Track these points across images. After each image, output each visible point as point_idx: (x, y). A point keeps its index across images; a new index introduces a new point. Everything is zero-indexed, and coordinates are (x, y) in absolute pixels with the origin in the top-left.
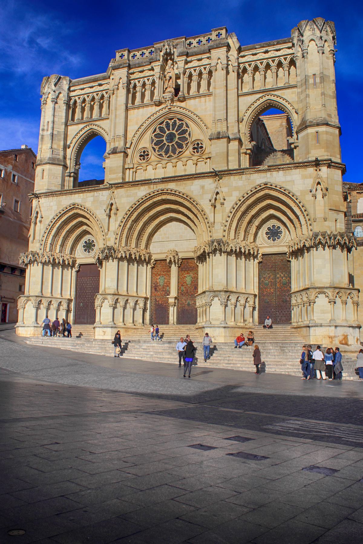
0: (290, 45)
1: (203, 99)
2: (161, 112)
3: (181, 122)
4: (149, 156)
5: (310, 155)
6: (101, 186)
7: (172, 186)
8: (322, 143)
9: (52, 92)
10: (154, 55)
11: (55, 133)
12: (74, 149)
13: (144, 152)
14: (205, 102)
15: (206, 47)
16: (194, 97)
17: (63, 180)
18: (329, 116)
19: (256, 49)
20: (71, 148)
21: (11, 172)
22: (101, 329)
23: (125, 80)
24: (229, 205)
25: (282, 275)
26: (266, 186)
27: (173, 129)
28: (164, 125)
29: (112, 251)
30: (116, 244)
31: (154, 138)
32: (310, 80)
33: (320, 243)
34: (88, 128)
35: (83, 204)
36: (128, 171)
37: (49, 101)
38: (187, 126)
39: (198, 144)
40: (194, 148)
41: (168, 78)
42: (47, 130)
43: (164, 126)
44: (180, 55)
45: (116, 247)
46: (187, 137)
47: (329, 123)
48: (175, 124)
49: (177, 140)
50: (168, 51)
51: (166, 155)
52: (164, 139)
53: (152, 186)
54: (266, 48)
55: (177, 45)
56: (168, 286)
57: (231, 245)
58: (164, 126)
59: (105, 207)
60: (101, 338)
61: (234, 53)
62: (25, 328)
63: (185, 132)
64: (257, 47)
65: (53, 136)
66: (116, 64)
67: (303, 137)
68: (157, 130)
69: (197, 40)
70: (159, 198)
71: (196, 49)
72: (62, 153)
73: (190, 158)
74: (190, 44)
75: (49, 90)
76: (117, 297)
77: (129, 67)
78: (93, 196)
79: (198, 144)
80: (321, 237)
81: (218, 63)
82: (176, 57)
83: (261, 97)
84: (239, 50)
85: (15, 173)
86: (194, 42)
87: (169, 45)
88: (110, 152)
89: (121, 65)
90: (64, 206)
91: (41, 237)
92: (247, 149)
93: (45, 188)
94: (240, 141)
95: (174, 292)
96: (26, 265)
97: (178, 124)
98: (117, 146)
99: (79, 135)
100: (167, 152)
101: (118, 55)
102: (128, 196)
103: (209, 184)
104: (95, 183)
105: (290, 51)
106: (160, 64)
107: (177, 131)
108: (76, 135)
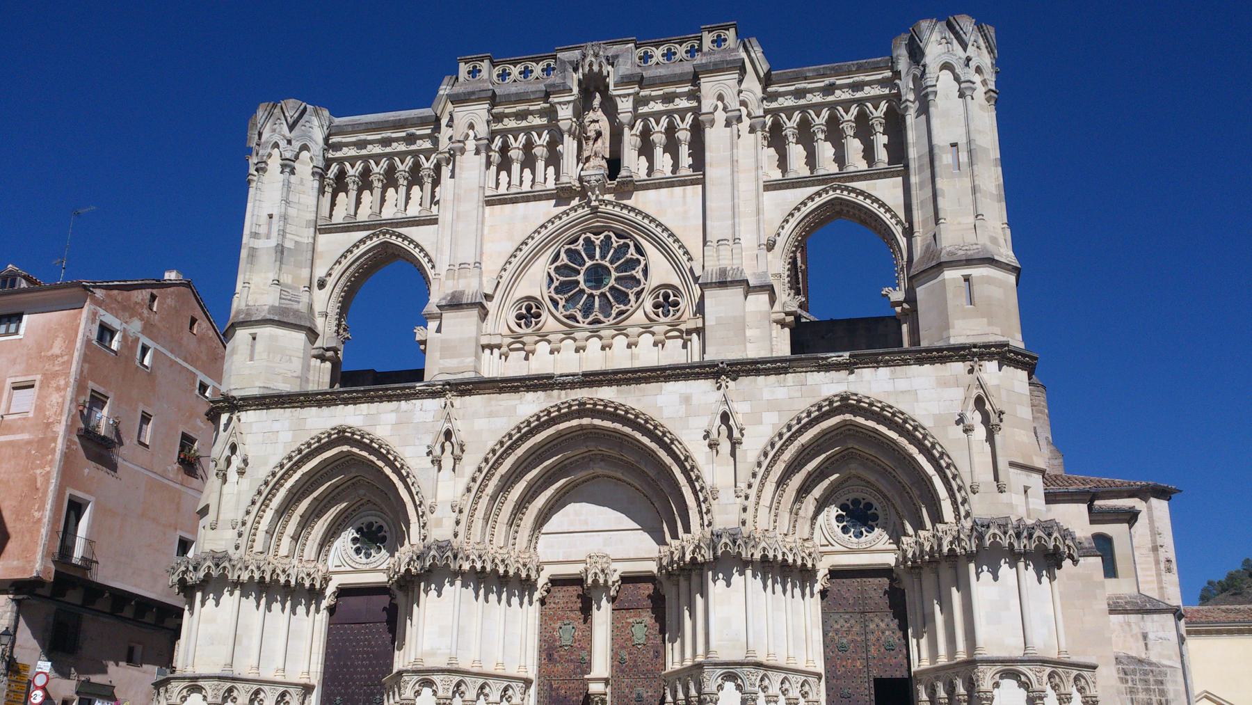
0: (888, 74)
2: (572, 214)
3: (622, 241)
4: (543, 318)
5: (952, 332)
6: (419, 386)
7: (607, 393)
8: (982, 305)
9: (283, 144)
10: (555, 78)
11: (288, 244)
12: (337, 290)
13: (529, 309)
14: (684, 197)
15: (688, 67)
17: (306, 368)
18: (994, 240)
20: (329, 287)
21: (137, 339)
23: (482, 130)
24: (754, 444)
25: (883, 625)
26: (846, 404)
27: (603, 257)
28: (579, 246)
29: (449, 553)
30: (456, 535)
31: (553, 274)
32: (944, 156)
33: (995, 545)
34: (376, 241)
35: (367, 429)
36: (487, 351)
37: (274, 164)
38: (639, 250)
40: (656, 306)
41: (592, 134)
42: (268, 237)
43: (580, 248)
44: (625, 81)
45: (456, 543)
46: (640, 276)
47: (996, 258)
48: (607, 243)
49: (612, 282)
50: (596, 68)
51: (585, 316)
52: (581, 278)
53: (556, 392)
54: (832, 80)
55: (616, 57)
56: (583, 649)
57: (763, 544)
58: (580, 248)
59: (429, 440)
61: (752, 85)
65: (282, 252)
66: (458, 89)
68: (563, 255)
69: (663, 49)
70: (575, 422)
71: (662, 71)
72: (305, 298)
73: (647, 329)
74: (646, 58)
75: (276, 138)
76: (456, 679)
77: (494, 100)
78: (397, 411)
79: (666, 297)
80: (997, 531)
81: (716, 108)
82: (611, 87)
83: (819, 194)
84: (766, 81)
85: (148, 342)
86: (658, 53)
87: (596, 55)
88: (443, 303)
89: (473, 93)
90: (314, 434)
91: (243, 512)
92: (787, 314)
94: (770, 289)
95: (601, 665)
96: (187, 590)
97: (615, 245)
98: (460, 288)
99: (351, 258)
100: (587, 311)
101: (463, 69)
102: (491, 415)
103: (702, 389)
104: (399, 378)
106: (572, 98)
107: (612, 262)
108: (344, 256)
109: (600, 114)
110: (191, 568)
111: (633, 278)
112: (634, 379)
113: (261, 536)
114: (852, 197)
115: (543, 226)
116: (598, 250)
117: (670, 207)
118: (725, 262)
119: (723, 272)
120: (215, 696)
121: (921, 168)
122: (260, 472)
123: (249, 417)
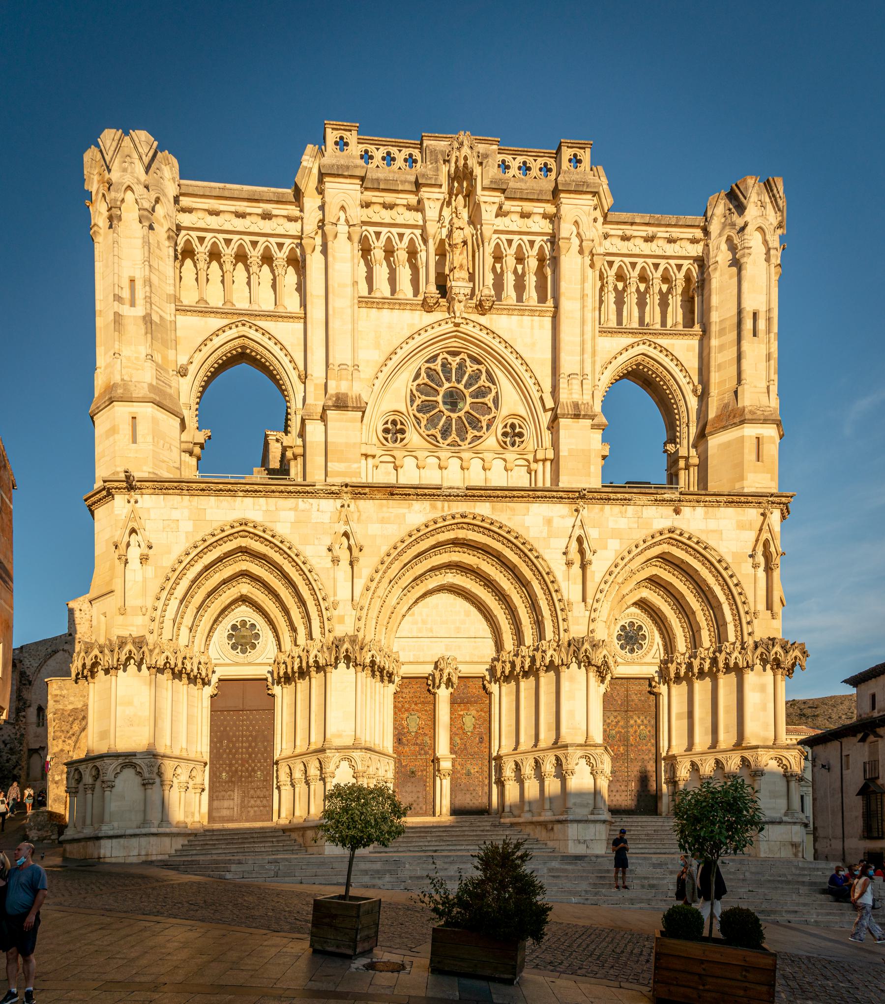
1: (526, 319)
16: (510, 311)
19: (632, 224)
29: (357, 647)
35: (268, 525)
42: (133, 304)
57: (605, 652)
62: (122, 841)
64: (637, 221)
90: (216, 525)
93: (145, 468)
105: (696, 250)
110: (106, 651)
113: (168, 624)
116: (466, 377)
120: (151, 772)
121: (722, 332)
122: (169, 561)
123: (147, 501)
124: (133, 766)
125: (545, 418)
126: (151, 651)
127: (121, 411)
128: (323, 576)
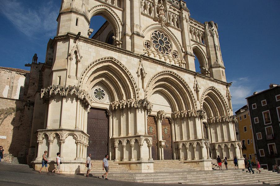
3: (166, 37)
7: (175, 71)
22: (146, 164)
34: (103, 7)
39: (175, 53)
52: (158, 41)
58: (157, 34)
60: (146, 171)
63: (167, 42)
67: (217, 71)
78: (127, 58)
102: (151, 68)
109: (162, 5)
111: (168, 46)
112: (180, 70)
114: (199, 47)
115: (152, 25)
117: (177, 34)
118: (190, 51)
119: (191, 53)
124: (74, 135)
125: (183, 54)
126: (80, 93)
127: (74, 16)
128: (135, 80)
